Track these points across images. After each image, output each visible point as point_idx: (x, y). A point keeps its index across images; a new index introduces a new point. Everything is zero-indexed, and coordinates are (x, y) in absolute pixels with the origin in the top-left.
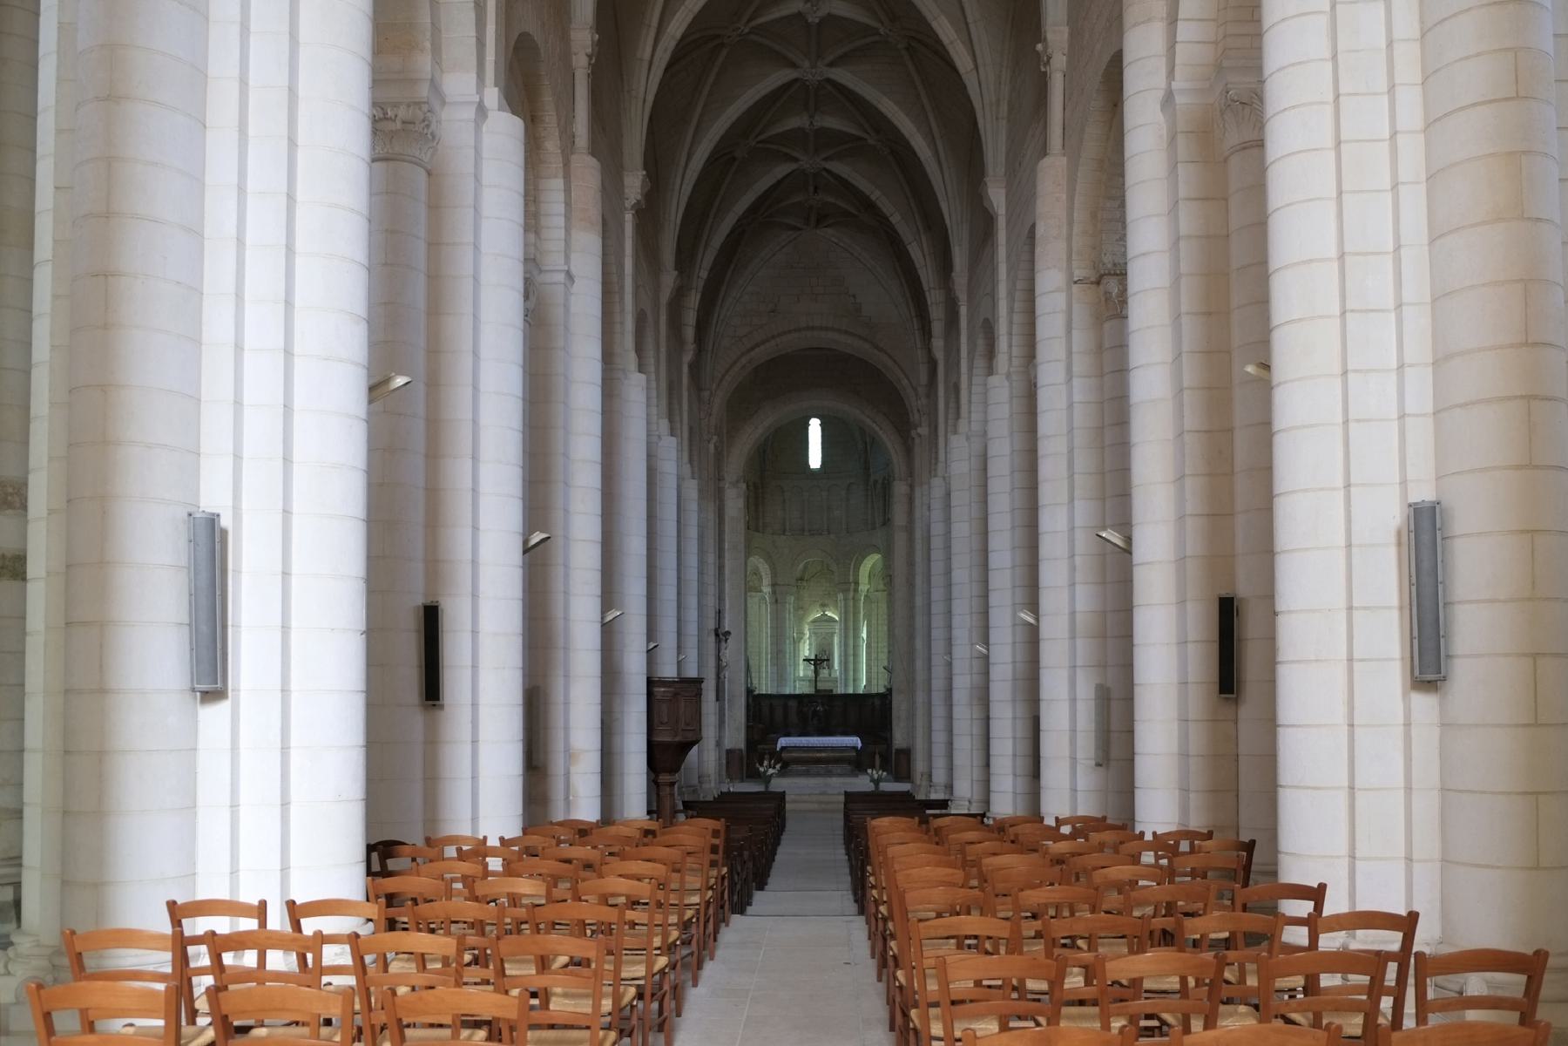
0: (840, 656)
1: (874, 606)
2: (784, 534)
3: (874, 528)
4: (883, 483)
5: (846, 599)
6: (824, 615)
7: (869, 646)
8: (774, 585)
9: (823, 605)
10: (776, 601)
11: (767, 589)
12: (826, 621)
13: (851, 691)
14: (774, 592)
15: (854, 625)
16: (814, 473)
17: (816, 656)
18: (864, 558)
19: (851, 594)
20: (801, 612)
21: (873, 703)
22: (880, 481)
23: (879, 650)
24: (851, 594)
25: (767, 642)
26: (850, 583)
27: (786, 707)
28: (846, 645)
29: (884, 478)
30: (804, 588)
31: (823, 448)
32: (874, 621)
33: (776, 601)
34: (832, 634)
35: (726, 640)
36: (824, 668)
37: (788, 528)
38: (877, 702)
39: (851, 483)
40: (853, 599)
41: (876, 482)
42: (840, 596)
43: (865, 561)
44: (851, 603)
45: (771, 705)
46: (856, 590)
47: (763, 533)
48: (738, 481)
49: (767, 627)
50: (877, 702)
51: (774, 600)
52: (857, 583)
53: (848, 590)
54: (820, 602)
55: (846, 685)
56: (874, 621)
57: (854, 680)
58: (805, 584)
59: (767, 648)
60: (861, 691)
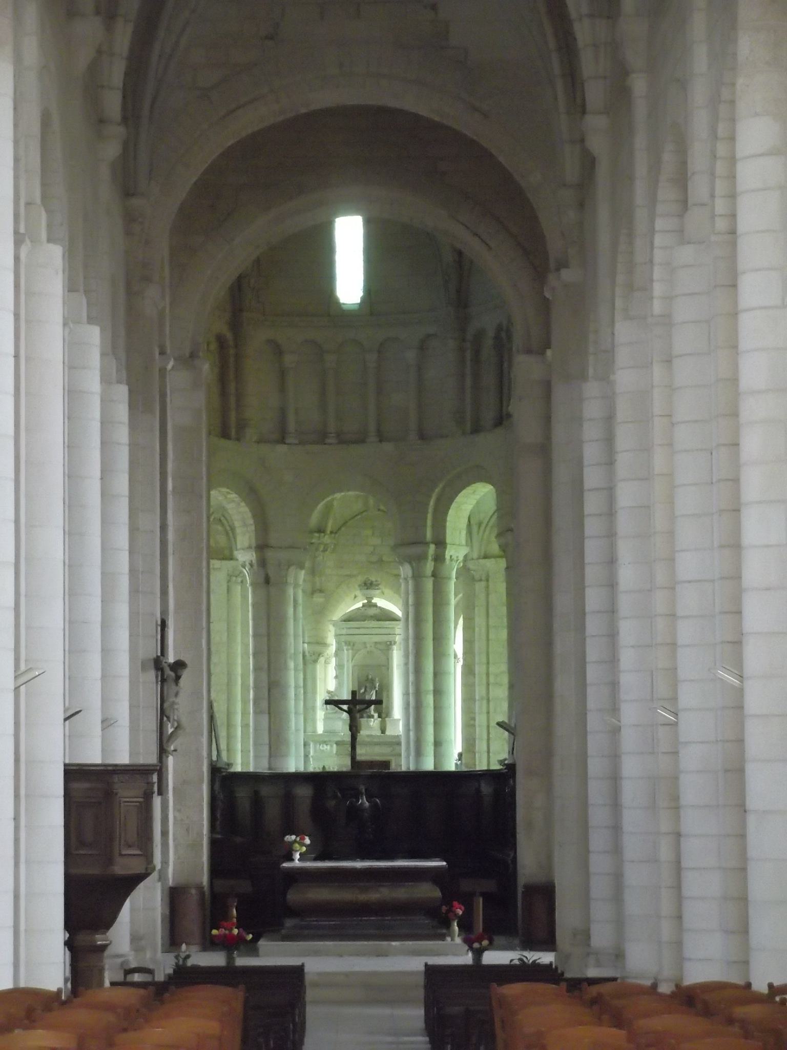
0: (406, 694)
1: (480, 587)
2: (282, 440)
3: (476, 429)
4: (497, 338)
5: (417, 577)
6: (370, 605)
7: (468, 670)
8: (261, 547)
9: (368, 585)
10: (267, 581)
11: (245, 556)
13: (429, 765)
14: (262, 563)
15: (434, 633)
17: (354, 693)
19: (429, 566)
20: (318, 599)
21: (478, 791)
22: (491, 334)
23: (492, 680)
24: (429, 566)
25: (245, 666)
26: (427, 544)
27: (288, 800)
28: (418, 671)
29: (499, 328)
30: (325, 550)
32: (479, 621)
33: (267, 581)
34: (388, 647)
35: (178, 678)
36: (372, 717)
37: (292, 426)
38: (486, 789)
39: (429, 336)
40: (434, 575)
41: (479, 335)
42: (406, 570)
43: (460, 498)
44: (429, 585)
45: (256, 793)
46: (439, 558)
47: (238, 439)
48: (193, 356)
49: (245, 633)
50: (486, 789)
51: (261, 579)
52: (441, 543)
53: (422, 558)
54: (360, 579)
55: (419, 753)
56: (479, 621)
57: (438, 744)
58: (327, 539)
59: (244, 676)
60: (451, 765)
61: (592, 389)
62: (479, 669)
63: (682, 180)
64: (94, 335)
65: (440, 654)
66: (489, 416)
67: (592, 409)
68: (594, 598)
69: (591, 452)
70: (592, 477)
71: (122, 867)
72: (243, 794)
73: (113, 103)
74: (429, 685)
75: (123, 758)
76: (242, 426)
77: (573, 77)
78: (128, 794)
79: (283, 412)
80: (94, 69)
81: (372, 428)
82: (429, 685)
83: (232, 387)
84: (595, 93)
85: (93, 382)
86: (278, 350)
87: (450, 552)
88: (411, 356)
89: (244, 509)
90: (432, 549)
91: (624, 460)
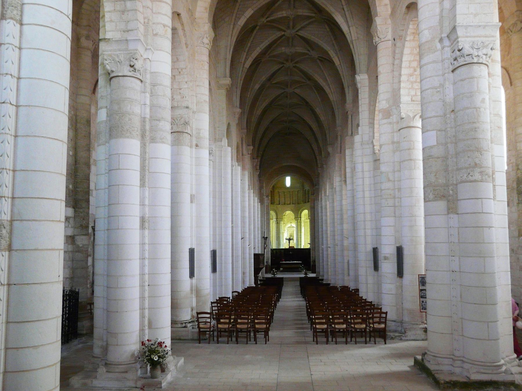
3: (305, 203)
6: (291, 225)
7: (305, 234)
8: (277, 219)
9: (291, 223)
10: (278, 223)
12: (292, 227)
13: (299, 247)
14: (277, 221)
16: (288, 188)
18: (303, 211)
19: (299, 221)
20: (284, 225)
22: (307, 190)
24: (299, 221)
31: (291, 180)
32: (306, 228)
33: (278, 223)
34: (294, 231)
44: (299, 223)
46: (300, 220)
48: (268, 196)
52: (301, 218)
53: (298, 220)
55: (298, 246)
56: (306, 228)
57: (300, 245)
58: (285, 217)
60: (302, 247)
61: (320, 203)
62: (306, 234)
63: (330, 179)
64: (256, 199)
65: (301, 232)
66: (307, 201)
67: (320, 206)
68: (320, 230)
69: (320, 211)
70: (320, 214)
71: (261, 267)
72: (274, 251)
73: (258, 167)
74: (299, 237)
75: (260, 253)
76: (274, 203)
77: (317, 161)
78: (261, 258)
79: (279, 200)
80: (256, 165)
81: (291, 202)
82: (299, 237)
83: (273, 197)
84: (319, 165)
85: (256, 205)
86: (279, 192)
87: (302, 219)
88: (296, 193)
89: (274, 213)
90: (299, 219)
91: (324, 214)
